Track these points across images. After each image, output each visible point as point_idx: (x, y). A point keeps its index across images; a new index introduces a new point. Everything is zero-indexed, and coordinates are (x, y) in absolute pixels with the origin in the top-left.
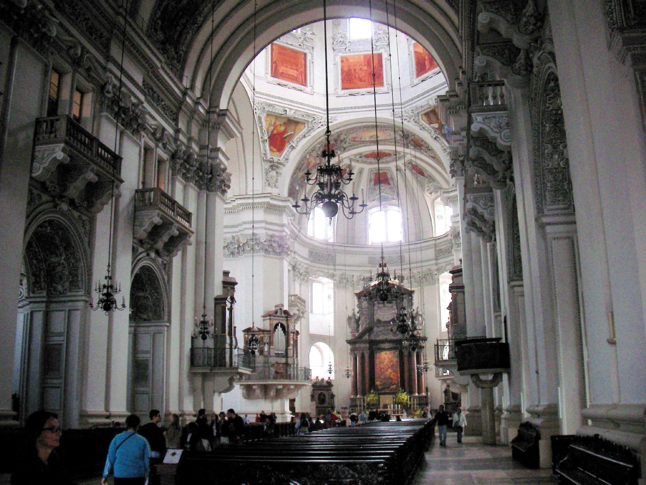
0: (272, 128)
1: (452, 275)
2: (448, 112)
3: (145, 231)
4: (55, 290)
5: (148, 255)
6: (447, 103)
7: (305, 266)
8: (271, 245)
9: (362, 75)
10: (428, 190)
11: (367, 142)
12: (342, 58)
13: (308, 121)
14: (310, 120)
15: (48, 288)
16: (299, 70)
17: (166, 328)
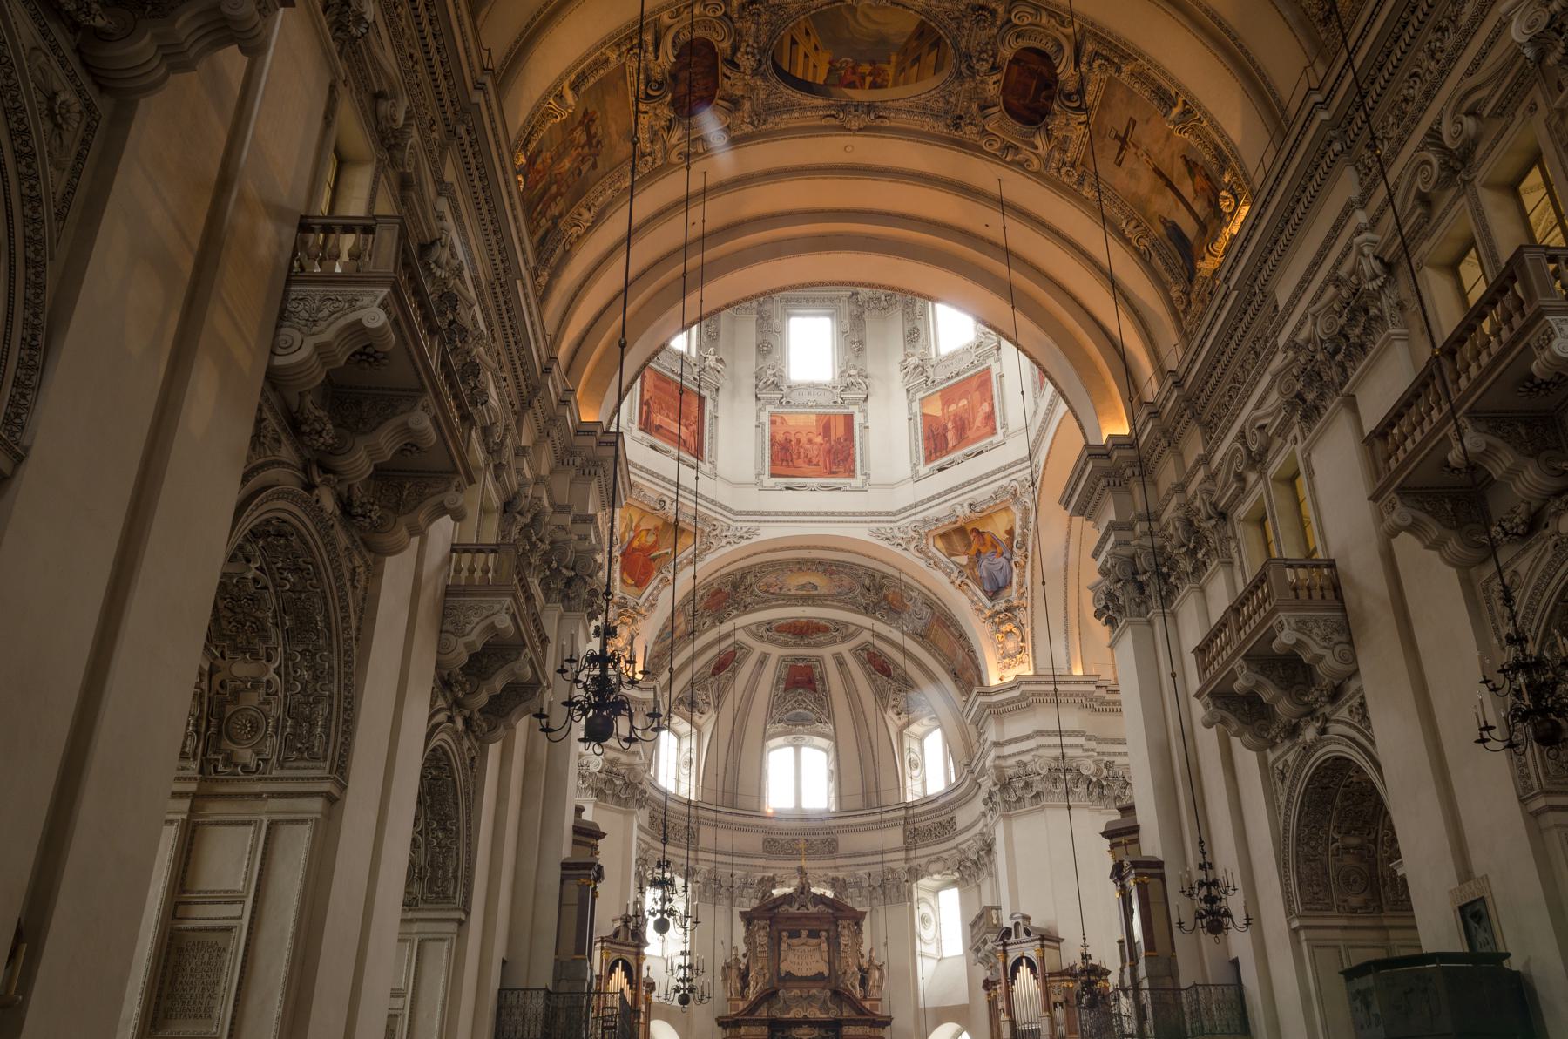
0: (632, 534)
1: (1107, 842)
2: (1103, 482)
3: (467, 645)
4: (229, 760)
5: (451, 719)
6: (1104, 463)
7: (643, 846)
8: (611, 781)
9: (813, 451)
10: (894, 706)
11: (790, 597)
12: (772, 414)
13: (703, 531)
14: (707, 530)
15: (204, 754)
16: (691, 428)
17: (453, 927)
